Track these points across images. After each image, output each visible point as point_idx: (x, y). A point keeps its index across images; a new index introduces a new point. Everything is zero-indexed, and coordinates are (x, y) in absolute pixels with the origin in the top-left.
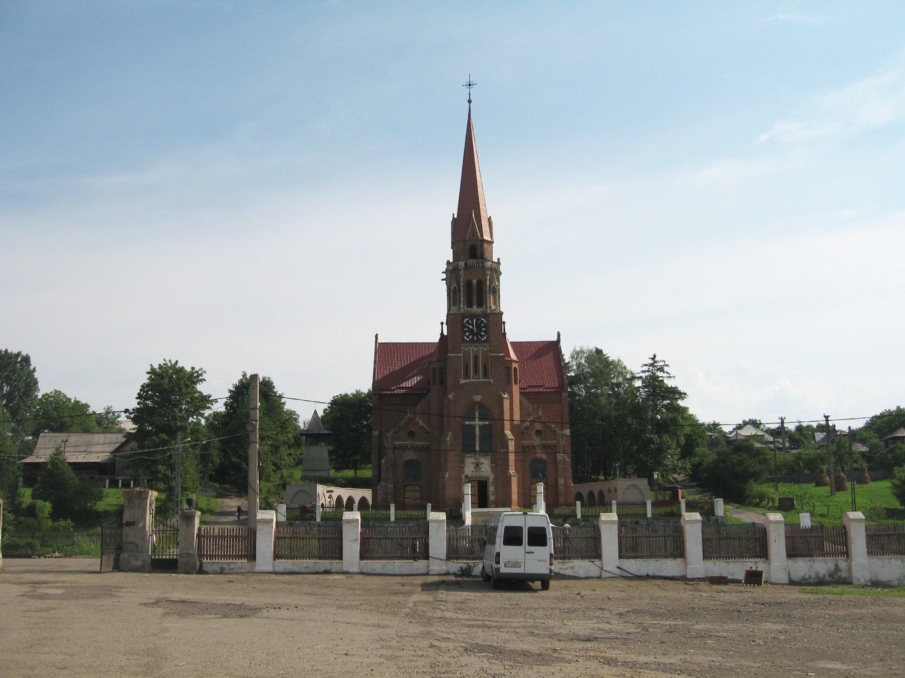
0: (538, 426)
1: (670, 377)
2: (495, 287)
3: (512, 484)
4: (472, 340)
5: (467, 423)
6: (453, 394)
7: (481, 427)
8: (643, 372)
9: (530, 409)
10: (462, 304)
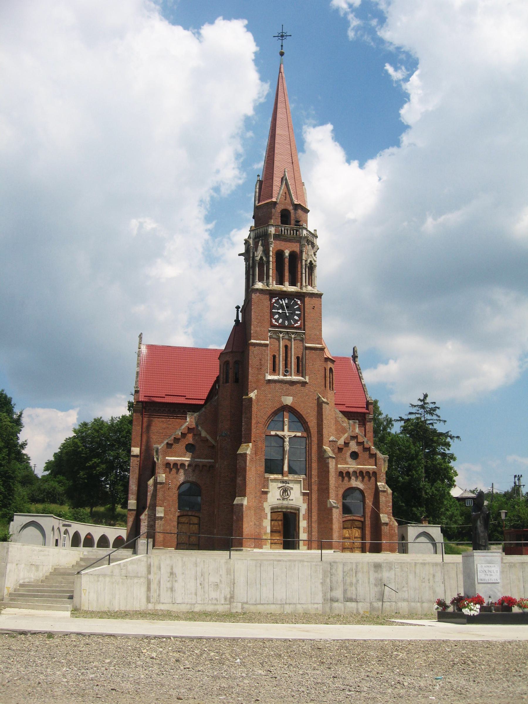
0: (353, 446)
1: (440, 420)
2: (313, 262)
3: (334, 517)
4: (282, 326)
5: (273, 433)
6: (256, 391)
8: (411, 413)
9: (345, 425)
10: (271, 278)
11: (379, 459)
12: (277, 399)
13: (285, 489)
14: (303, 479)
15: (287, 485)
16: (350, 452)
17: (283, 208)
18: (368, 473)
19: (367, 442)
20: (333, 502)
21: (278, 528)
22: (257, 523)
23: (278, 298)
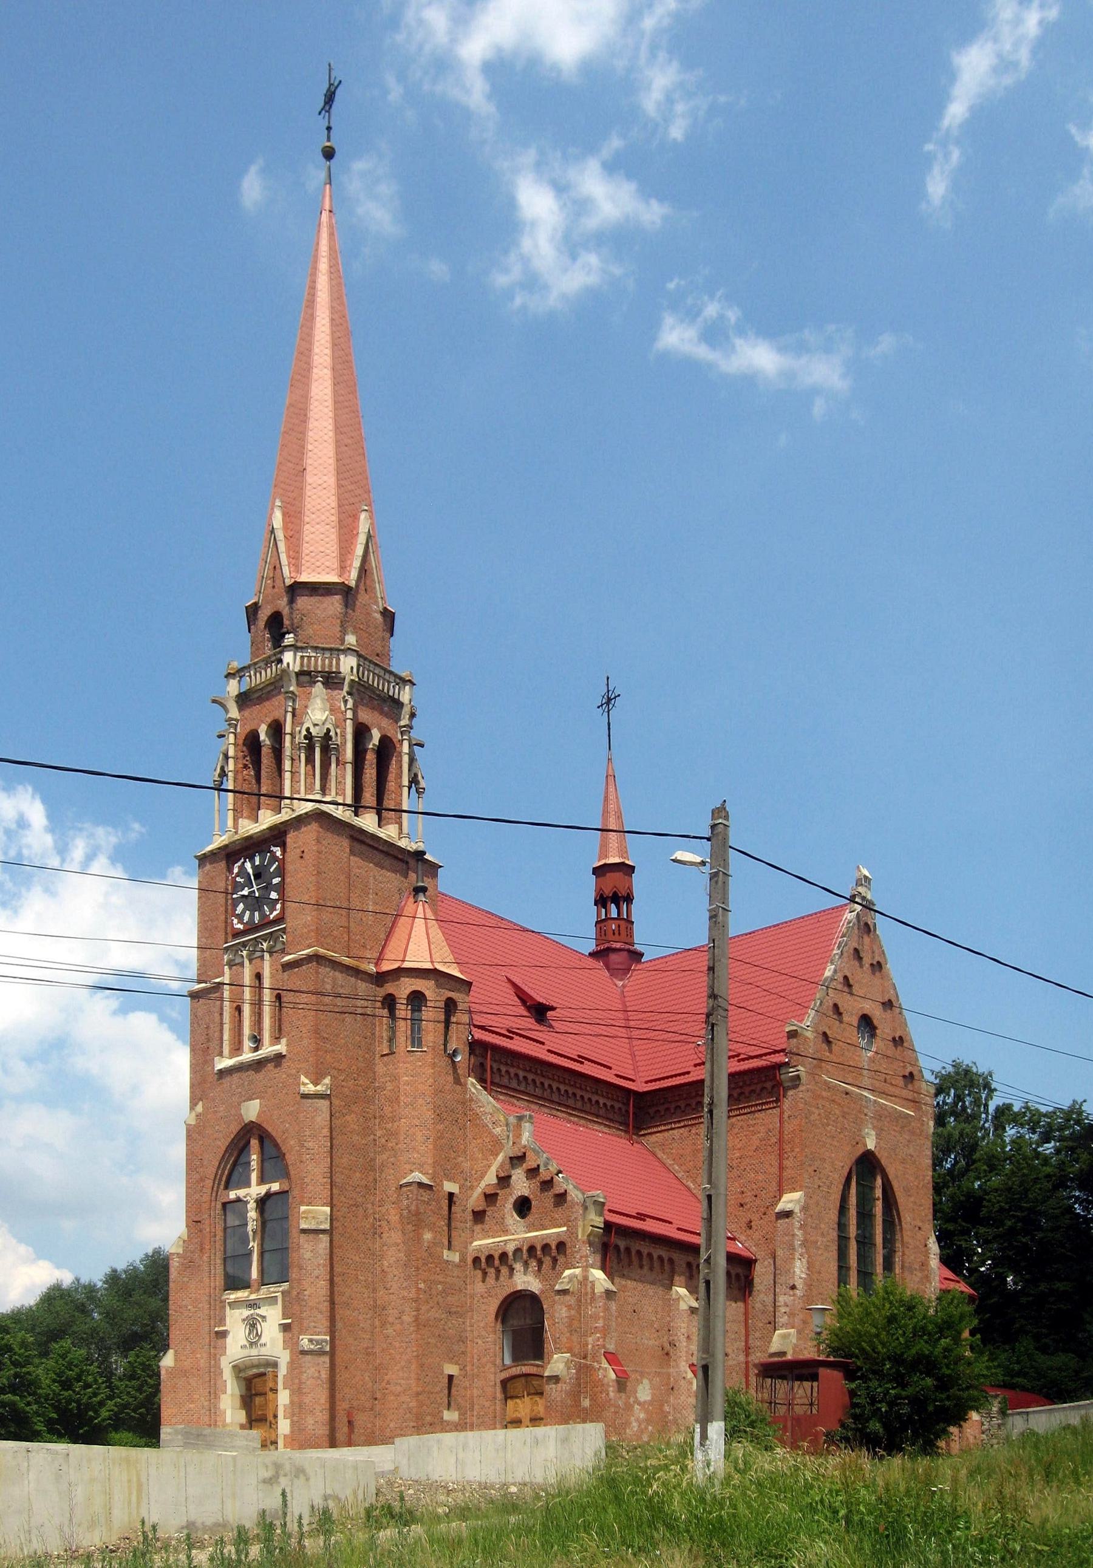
0: (521, 1185)
5: (232, 1195)
7: (262, 1202)
11: (574, 1204)
12: (233, 1112)
14: (283, 1292)
16: (512, 1200)
17: (269, 614)
18: (546, 1247)
19: (546, 1165)
23: (242, 860)
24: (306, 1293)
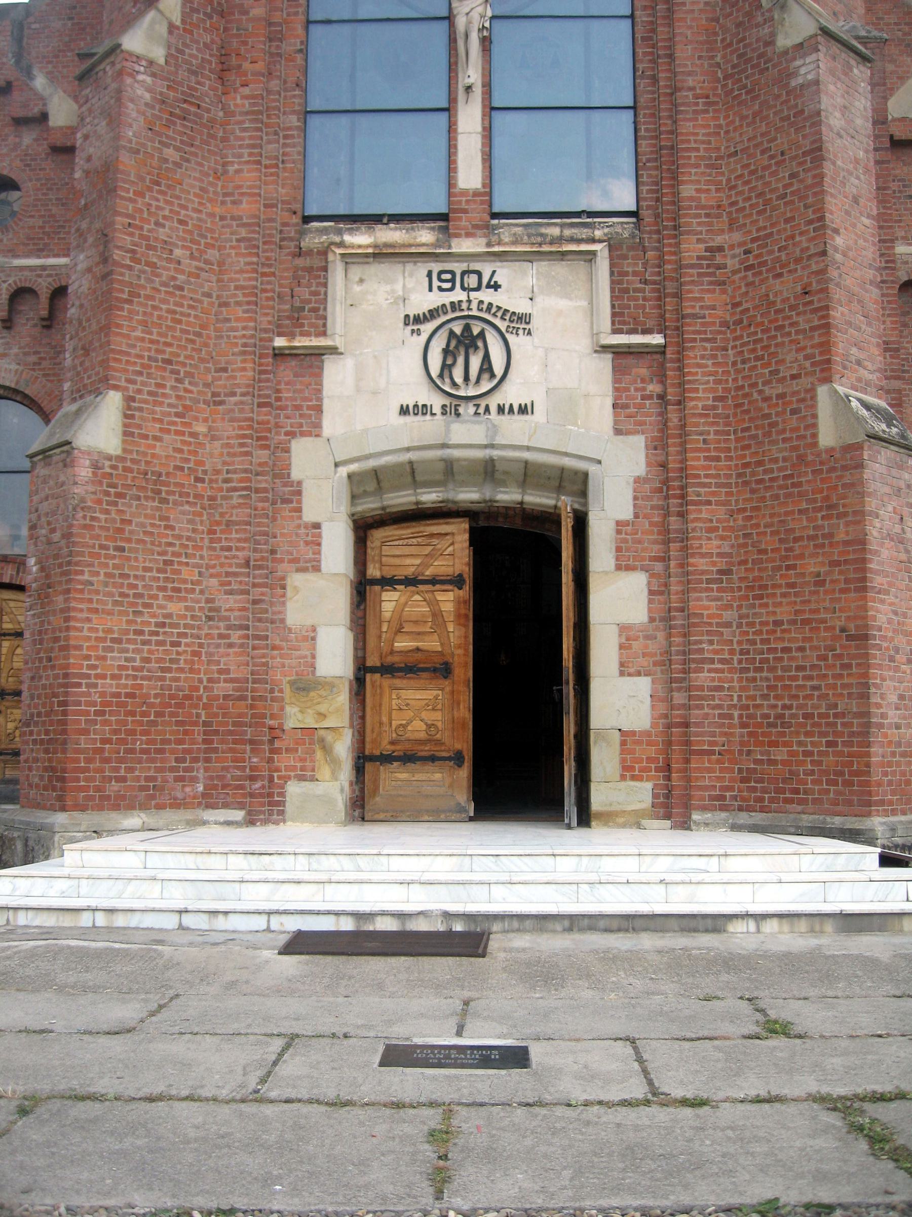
3: (874, 530)
13: (467, 328)
15: (487, 296)
20: (867, 407)
21: (432, 644)
22: (228, 603)
24: (839, 241)
